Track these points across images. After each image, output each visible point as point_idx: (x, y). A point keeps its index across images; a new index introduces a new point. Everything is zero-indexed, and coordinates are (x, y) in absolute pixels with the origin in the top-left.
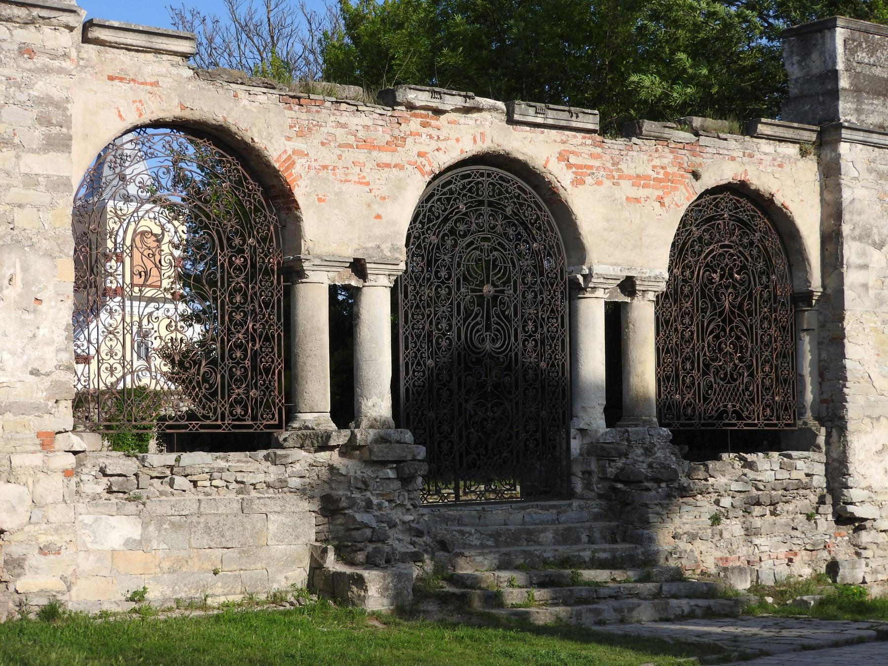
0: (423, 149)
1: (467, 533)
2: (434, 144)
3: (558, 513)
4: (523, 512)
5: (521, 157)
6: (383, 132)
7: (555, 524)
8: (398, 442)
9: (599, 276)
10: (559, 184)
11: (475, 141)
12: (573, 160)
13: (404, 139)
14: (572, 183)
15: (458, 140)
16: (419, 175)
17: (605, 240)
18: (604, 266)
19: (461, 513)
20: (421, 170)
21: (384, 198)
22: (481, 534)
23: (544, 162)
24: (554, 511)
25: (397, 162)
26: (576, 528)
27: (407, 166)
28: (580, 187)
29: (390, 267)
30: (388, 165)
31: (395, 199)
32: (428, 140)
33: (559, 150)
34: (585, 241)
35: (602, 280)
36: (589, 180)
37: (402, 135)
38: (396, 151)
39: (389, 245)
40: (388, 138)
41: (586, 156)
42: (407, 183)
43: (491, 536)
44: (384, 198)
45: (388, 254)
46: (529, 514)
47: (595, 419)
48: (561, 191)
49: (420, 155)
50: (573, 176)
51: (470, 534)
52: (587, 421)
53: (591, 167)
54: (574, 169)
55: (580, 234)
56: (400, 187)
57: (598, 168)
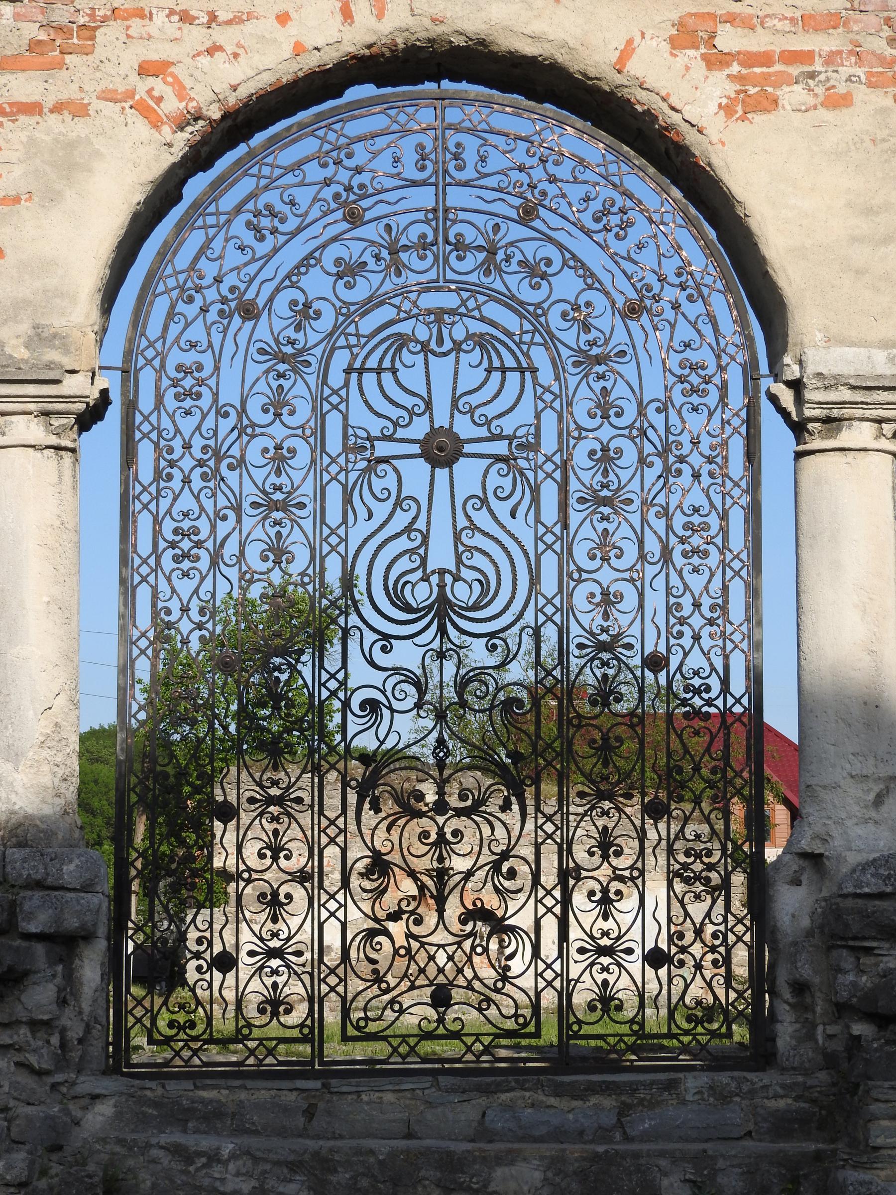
0: (155, 53)
1: (199, 1154)
2: (196, 36)
3: (623, 1110)
4: (483, 1101)
5: (529, 49)
6: (17, 17)
7: (610, 1140)
8: (40, 885)
9: (831, 382)
10: (676, 118)
11: (347, 14)
12: (729, 39)
13: (89, 31)
14: (727, 109)
15: (283, 19)
16: (140, 128)
17: (859, 272)
18: (850, 352)
19: (243, 1095)
20: (143, 110)
21: (17, 200)
22: (256, 1160)
23: (614, 57)
24: (609, 1102)
25: (64, 97)
26: (636, 1155)
27: (97, 104)
28: (757, 118)
29: (31, 389)
30: (33, 109)
31: (52, 197)
32: (172, 28)
33: (675, 16)
34: (781, 281)
35: (846, 395)
36: (793, 95)
37: (82, 20)
38: (61, 65)
39: (25, 328)
40: (31, 31)
41: (786, 25)
42: (97, 154)
43: (294, 1166)
44: (17, 200)
45: (21, 353)
46: (509, 1107)
47: (840, 823)
48: (691, 138)
49: (145, 70)
50: (731, 89)
51: (213, 1158)
52: (818, 828)
53: (806, 57)
54: (735, 68)
55: (764, 258)
56: (70, 163)
57: (831, 59)
